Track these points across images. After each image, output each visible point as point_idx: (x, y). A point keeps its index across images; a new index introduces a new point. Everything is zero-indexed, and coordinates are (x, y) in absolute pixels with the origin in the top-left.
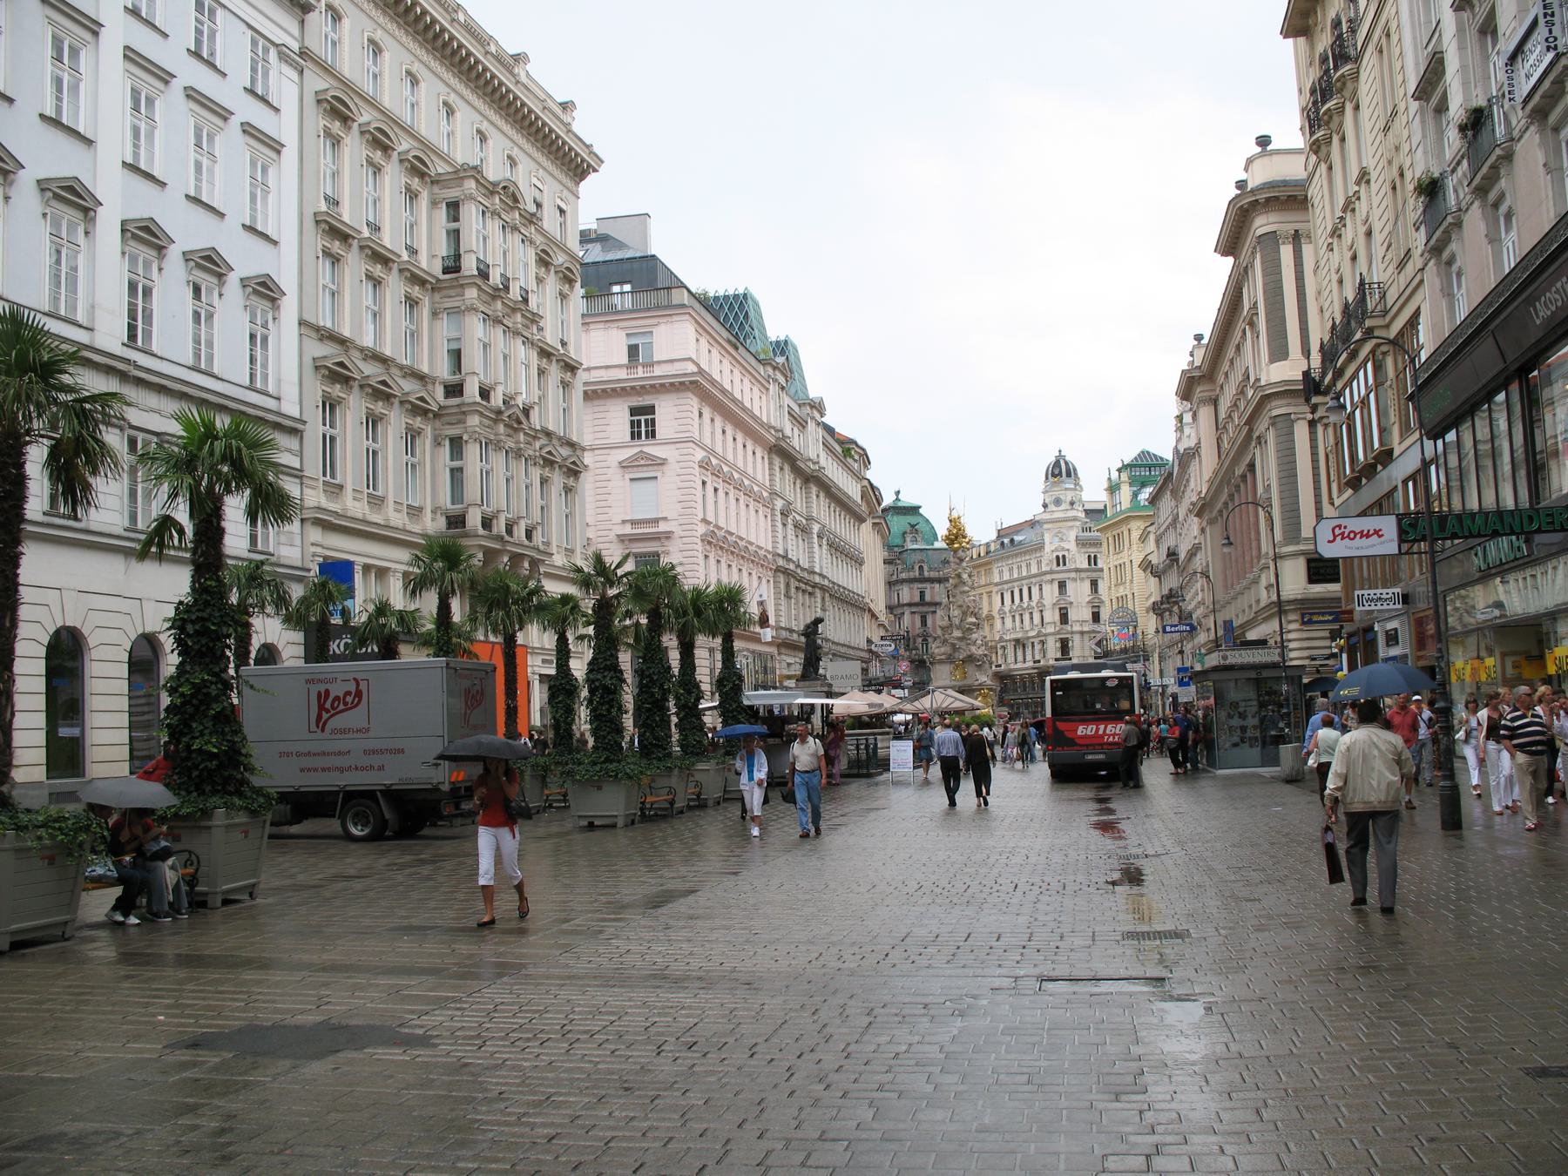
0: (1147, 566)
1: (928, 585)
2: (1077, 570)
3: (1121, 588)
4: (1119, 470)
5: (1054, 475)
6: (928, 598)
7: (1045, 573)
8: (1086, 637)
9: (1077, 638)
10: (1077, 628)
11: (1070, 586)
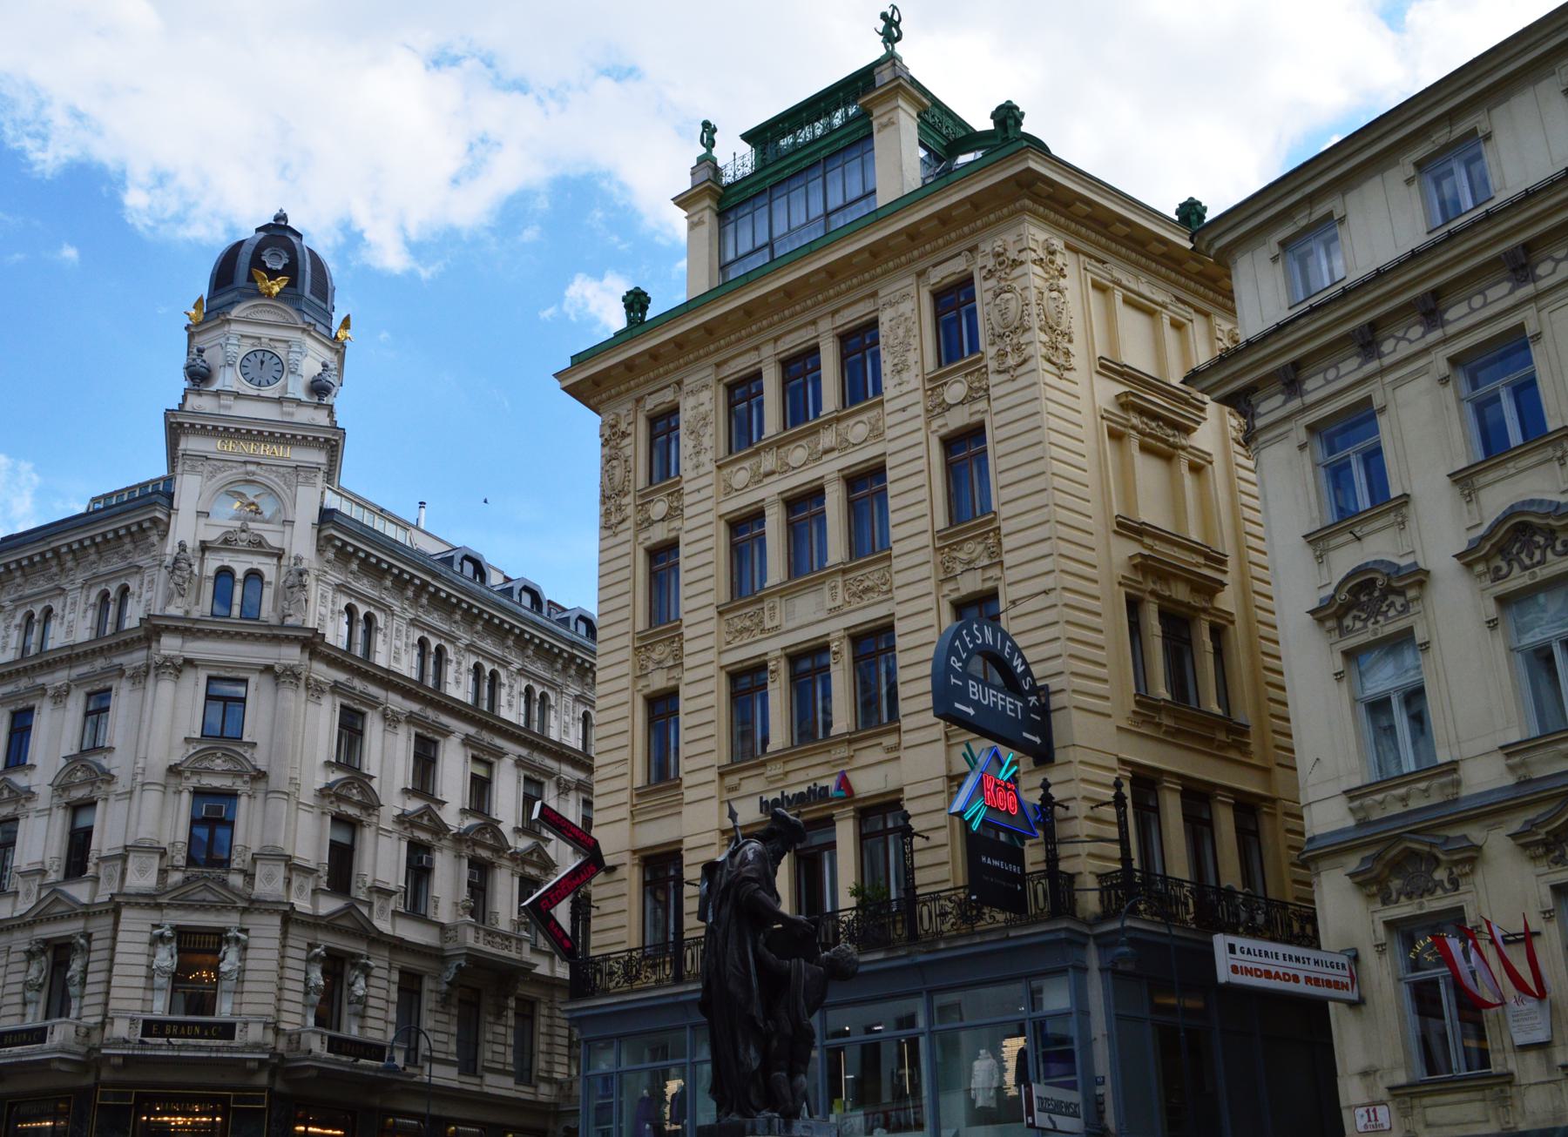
2: (312, 643)
7: (153, 629)
8: (299, 940)
9: (265, 931)
10: (270, 884)
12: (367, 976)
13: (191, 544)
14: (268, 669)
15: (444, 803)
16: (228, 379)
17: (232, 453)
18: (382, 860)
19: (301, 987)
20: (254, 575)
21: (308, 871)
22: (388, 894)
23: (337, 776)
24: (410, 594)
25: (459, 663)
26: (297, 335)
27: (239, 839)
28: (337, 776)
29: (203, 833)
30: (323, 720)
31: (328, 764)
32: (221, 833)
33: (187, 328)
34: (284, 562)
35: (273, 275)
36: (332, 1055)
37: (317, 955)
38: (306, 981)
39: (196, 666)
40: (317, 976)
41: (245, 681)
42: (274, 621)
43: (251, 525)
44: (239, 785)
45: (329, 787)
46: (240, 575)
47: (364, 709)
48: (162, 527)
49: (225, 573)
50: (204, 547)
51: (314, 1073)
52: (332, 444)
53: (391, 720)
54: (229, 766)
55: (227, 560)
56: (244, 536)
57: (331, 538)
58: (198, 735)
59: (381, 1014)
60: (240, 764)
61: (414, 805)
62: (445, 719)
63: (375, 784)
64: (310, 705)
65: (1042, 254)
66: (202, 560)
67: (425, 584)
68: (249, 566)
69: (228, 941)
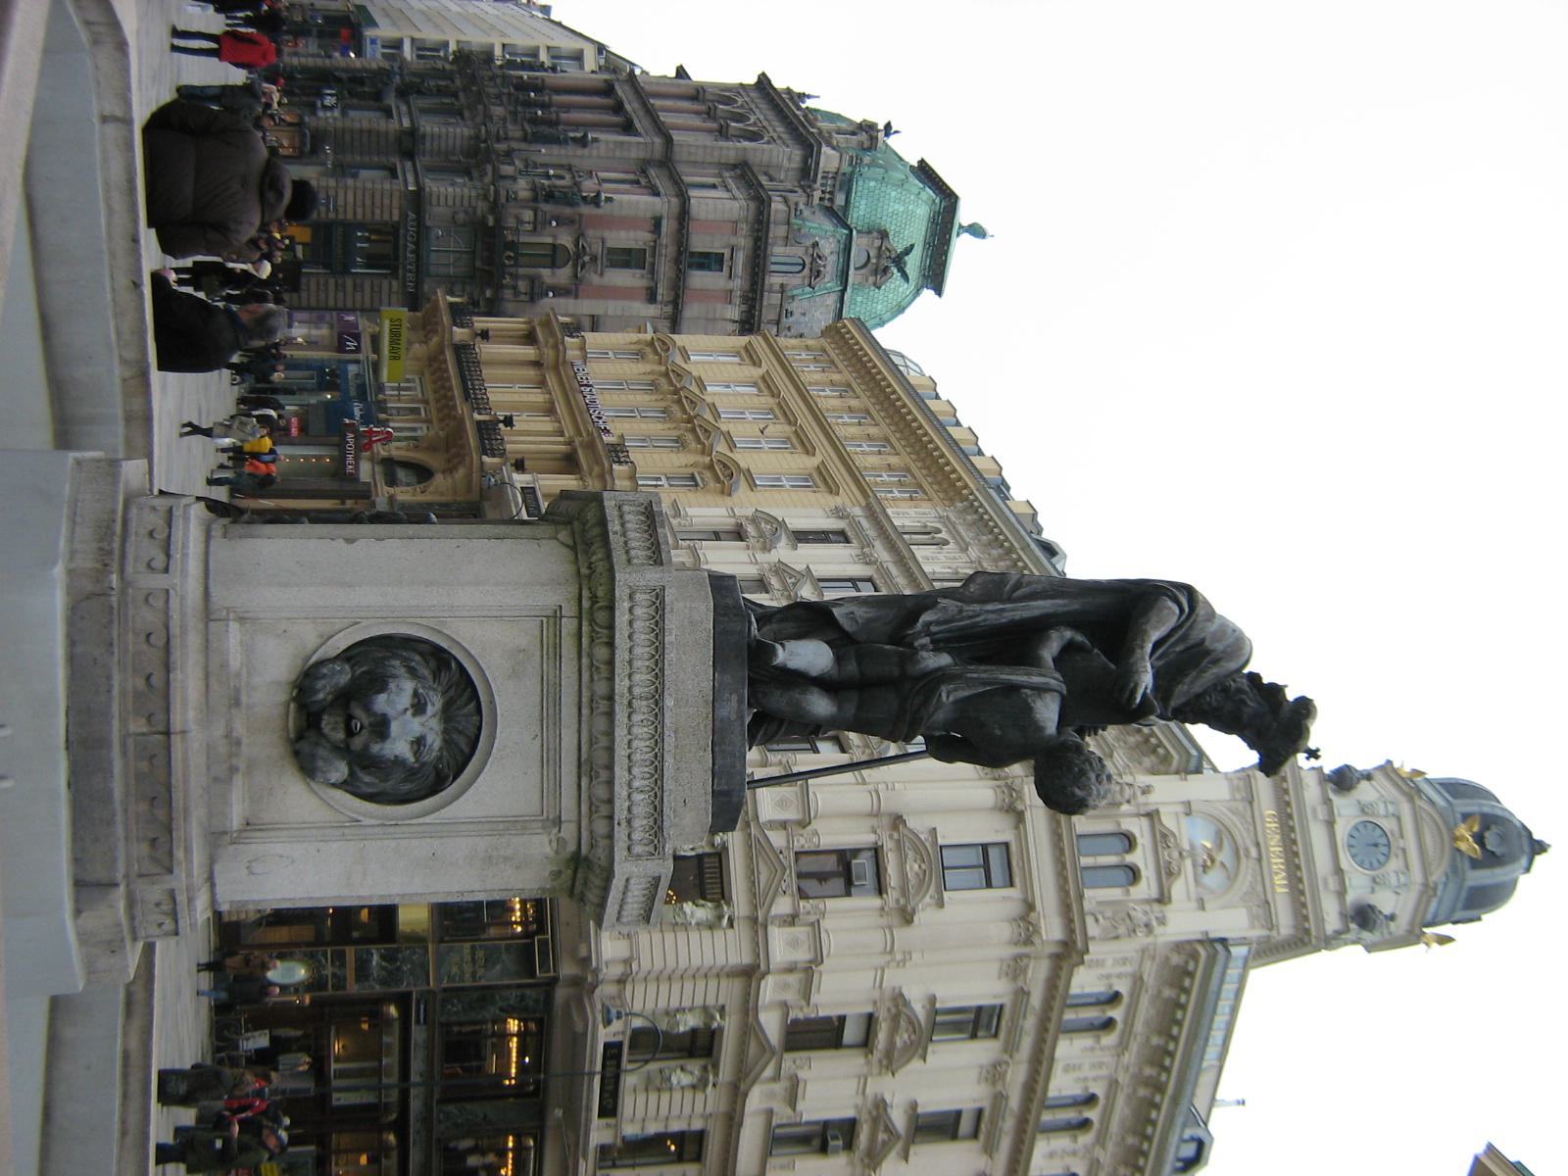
1: (738, 284)
2: (1069, 952)
6: (699, 279)
8: (728, 993)
9: (729, 948)
10: (782, 946)
12: (694, 1087)
13: (1153, 798)
14: (1030, 906)
15: (906, 1159)
16: (1346, 808)
17: (1264, 829)
18: (830, 1087)
19: (674, 1003)
20: (1134, 874)
21: (806, 993)
22: (792, 1099)
23: (919, 1009)
24: (1148, 1071)
25: (1074, 1153)
26: (1417, 876)
27: (831, 904)
28: (919, 1009)
29: (830, 864)
30: (982, 987)
31: (933, 999)
32: (838, 884)
33: (1389, 762)
34: (1156, 907)
35: (1479, 839)
36: (600, 1049)
37: (713, 1018)
38: (681, 1010)
39: (1017, 827)
40: (689, 1022)
41: (1011, 883)
42: (1087, 906)
43: (1188, 863)
44: (892, 895)
45: (907, 1003)
47: (1002, 1034)
48: (1162, 768)
49: (1129, 841)
50: (1152, 816)
51: (579, 1028)
52: (1303, 941)
53: (994, 1073)
54: (913, 880)
55: (1143, 839)
56: (1175, 854)
58: (941, 842)
59: (652, 1111)
60: (918, 891)
61: (899, 1119)
62: (1005, 1144)
63: (916, 1064)
64: (996, 966)
66: (1138, 815)
67: (1160, 1088)
69: (719, 906)
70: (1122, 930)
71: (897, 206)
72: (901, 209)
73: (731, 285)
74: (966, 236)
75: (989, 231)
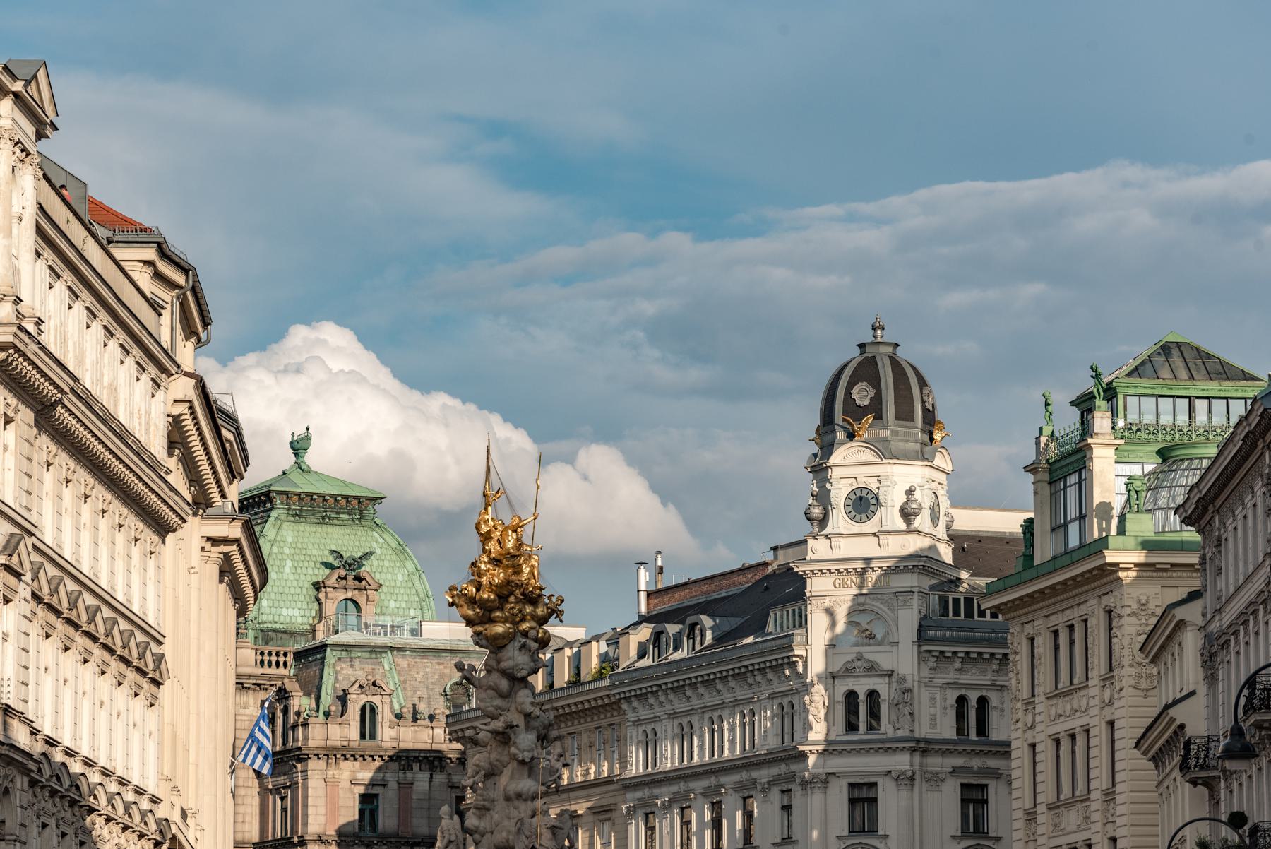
0: (1167, 745)
2: (923, 747)
3: (1072, 818)
4: (1085, 404)
5: (855, 412)
11: (891, 802)
20: (873, 695)
30: (948, 798)
42: (891, 734)
46: (862, 697)
47: (984, 782)
49: (851, 696)
56: (859, 663)
57: (930, 651)
58: (846, 833)
65: (1135, 606)
68: (867, 688)
70: (907, 710)
71: (287, 570)
72: (289, 563)
73: (393, 785)
74: (311, 458)
75: (300, 431)
